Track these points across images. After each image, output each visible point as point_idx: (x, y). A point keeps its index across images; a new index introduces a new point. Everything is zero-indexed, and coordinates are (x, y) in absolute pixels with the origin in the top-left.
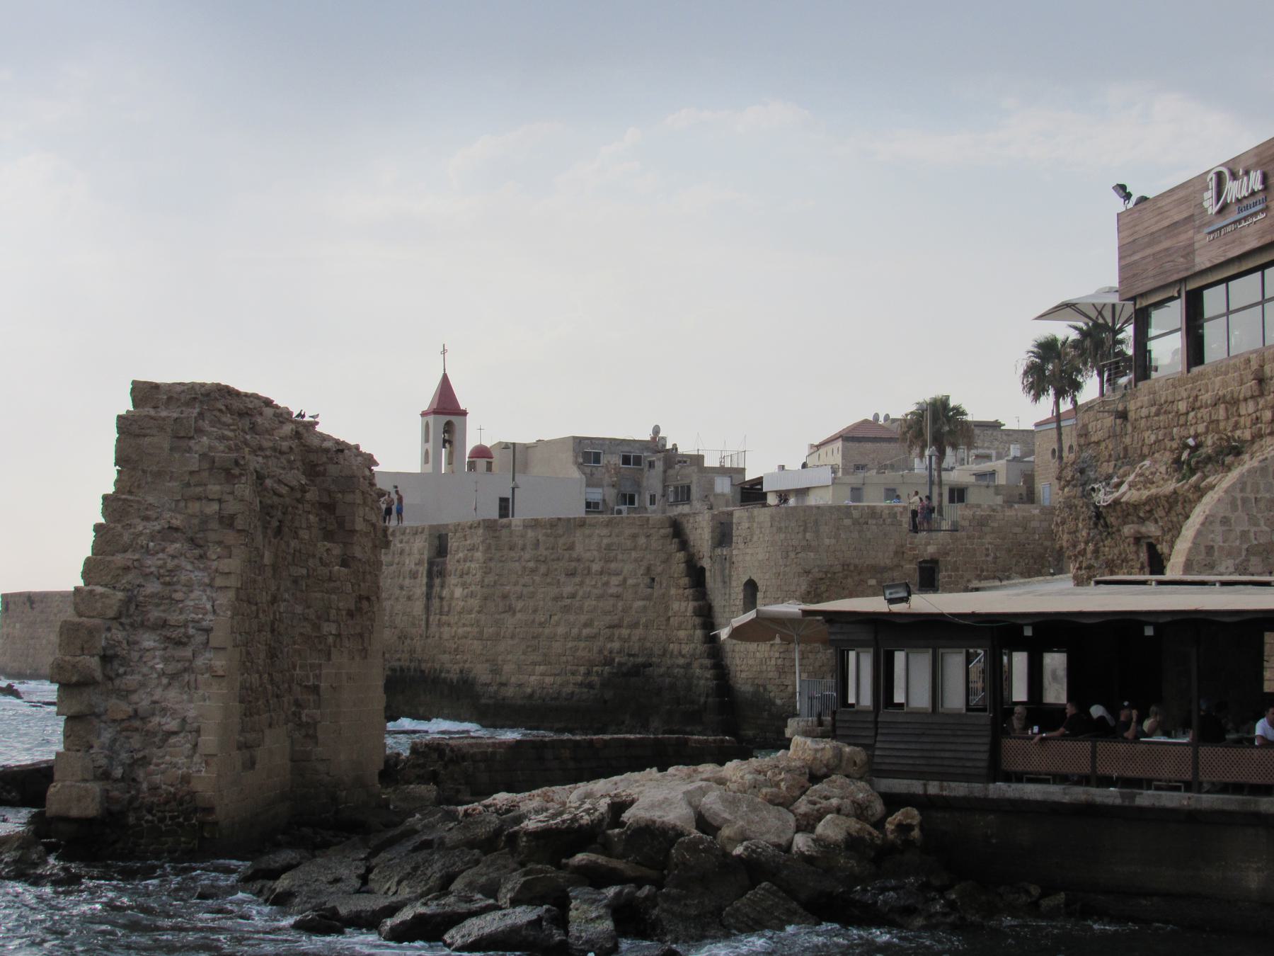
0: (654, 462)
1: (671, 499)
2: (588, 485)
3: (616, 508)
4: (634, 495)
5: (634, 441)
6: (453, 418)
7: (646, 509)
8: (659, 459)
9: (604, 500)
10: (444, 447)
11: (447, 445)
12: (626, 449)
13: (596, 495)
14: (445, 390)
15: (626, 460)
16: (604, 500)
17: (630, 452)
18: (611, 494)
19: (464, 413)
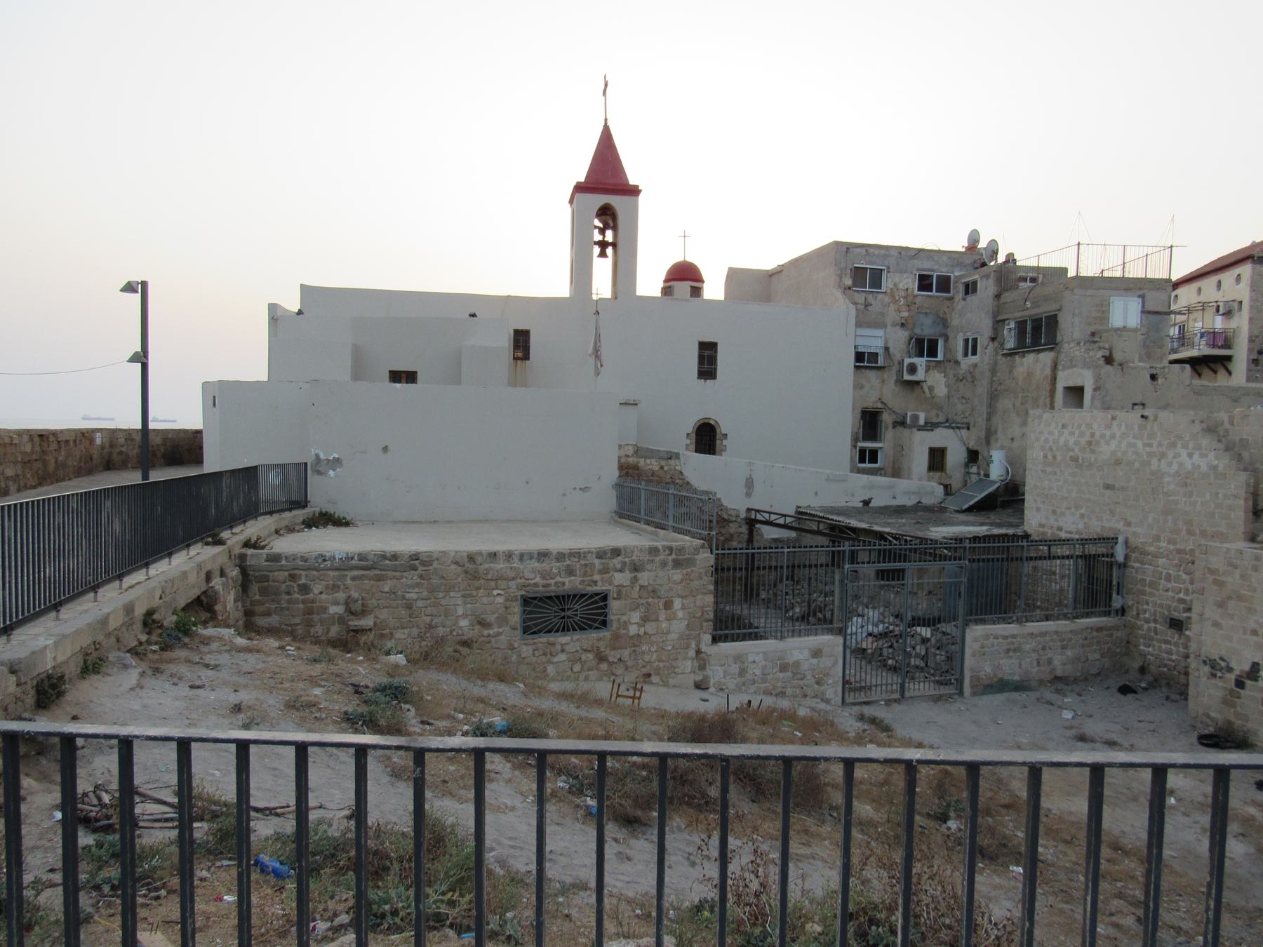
0: (975, 283)
1: (1011, 343)
2: (859, 324)
3: (907, 361)
4: (937, 340)
5: (939, 252)
6: (615, 201)
7: (957, 362)
8: (987, 277)
9: (887, 349)
10: (603, 254)
11: (609, 251)
12: (925, 265)
13: (873, 341)
14: (606, 154)
15: (925, 283)
16: (887, 349)
17: (933, 270)
18: (898, 340)
19: (634, 191)
